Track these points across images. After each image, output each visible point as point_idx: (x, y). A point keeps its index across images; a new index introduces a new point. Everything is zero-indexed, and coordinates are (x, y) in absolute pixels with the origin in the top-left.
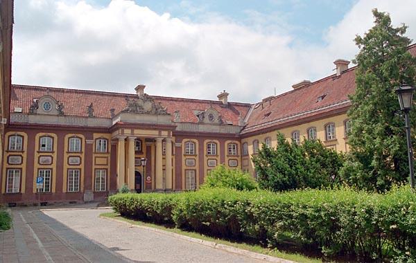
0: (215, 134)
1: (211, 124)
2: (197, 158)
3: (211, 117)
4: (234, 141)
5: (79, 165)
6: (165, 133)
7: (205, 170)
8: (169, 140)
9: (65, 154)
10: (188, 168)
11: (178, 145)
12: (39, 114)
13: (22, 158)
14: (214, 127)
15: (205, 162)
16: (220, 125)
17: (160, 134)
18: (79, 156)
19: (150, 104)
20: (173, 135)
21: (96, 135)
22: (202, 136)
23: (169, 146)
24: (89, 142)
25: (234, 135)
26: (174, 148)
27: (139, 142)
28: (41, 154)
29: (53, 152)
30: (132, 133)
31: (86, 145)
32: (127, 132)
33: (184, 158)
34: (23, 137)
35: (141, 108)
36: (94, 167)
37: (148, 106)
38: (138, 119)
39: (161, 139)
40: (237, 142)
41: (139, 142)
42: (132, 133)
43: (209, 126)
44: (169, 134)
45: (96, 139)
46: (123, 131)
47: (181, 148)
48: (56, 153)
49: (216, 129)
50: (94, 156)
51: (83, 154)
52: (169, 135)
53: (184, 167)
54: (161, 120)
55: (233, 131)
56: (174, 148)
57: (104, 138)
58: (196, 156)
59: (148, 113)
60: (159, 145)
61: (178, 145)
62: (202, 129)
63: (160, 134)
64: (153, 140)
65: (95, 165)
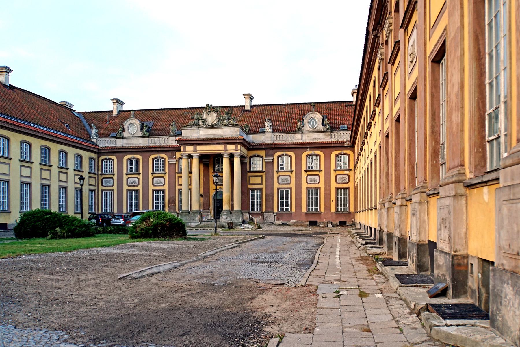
4: (345, 152)
5: (163, 185)
6: (231, 148)
10: (281, 186)
11: (269, 159)
12: (125, 138)
13: (113, 179)
14: (316, 135)
15: (293, 180)
16: (324, 132)
17: (226, 150)
18: (163, 177)
19: (215, 115)
23: (237, 162)
25: (343, 143)
26: (264, 163)
27: (204, 159)
28: (338, 173)
29: (320, 171)
30: (195, 151)
33: (276, 175)
34: (290, 156)
35: (204, 121)
37: (212, 118)
38: (203, 133)
40: (348, 152)
41: (204, 159)
42: (195, 151)
43: (311, 135)
44: (236, 147)
46: (185, 149)
48: (116, 175)
53: (276, 186)
56: (264, 163)
59: (212, 126)
60: (226, 162)
61: (269, 159)
62: (298, 138)
63: (226, 150)
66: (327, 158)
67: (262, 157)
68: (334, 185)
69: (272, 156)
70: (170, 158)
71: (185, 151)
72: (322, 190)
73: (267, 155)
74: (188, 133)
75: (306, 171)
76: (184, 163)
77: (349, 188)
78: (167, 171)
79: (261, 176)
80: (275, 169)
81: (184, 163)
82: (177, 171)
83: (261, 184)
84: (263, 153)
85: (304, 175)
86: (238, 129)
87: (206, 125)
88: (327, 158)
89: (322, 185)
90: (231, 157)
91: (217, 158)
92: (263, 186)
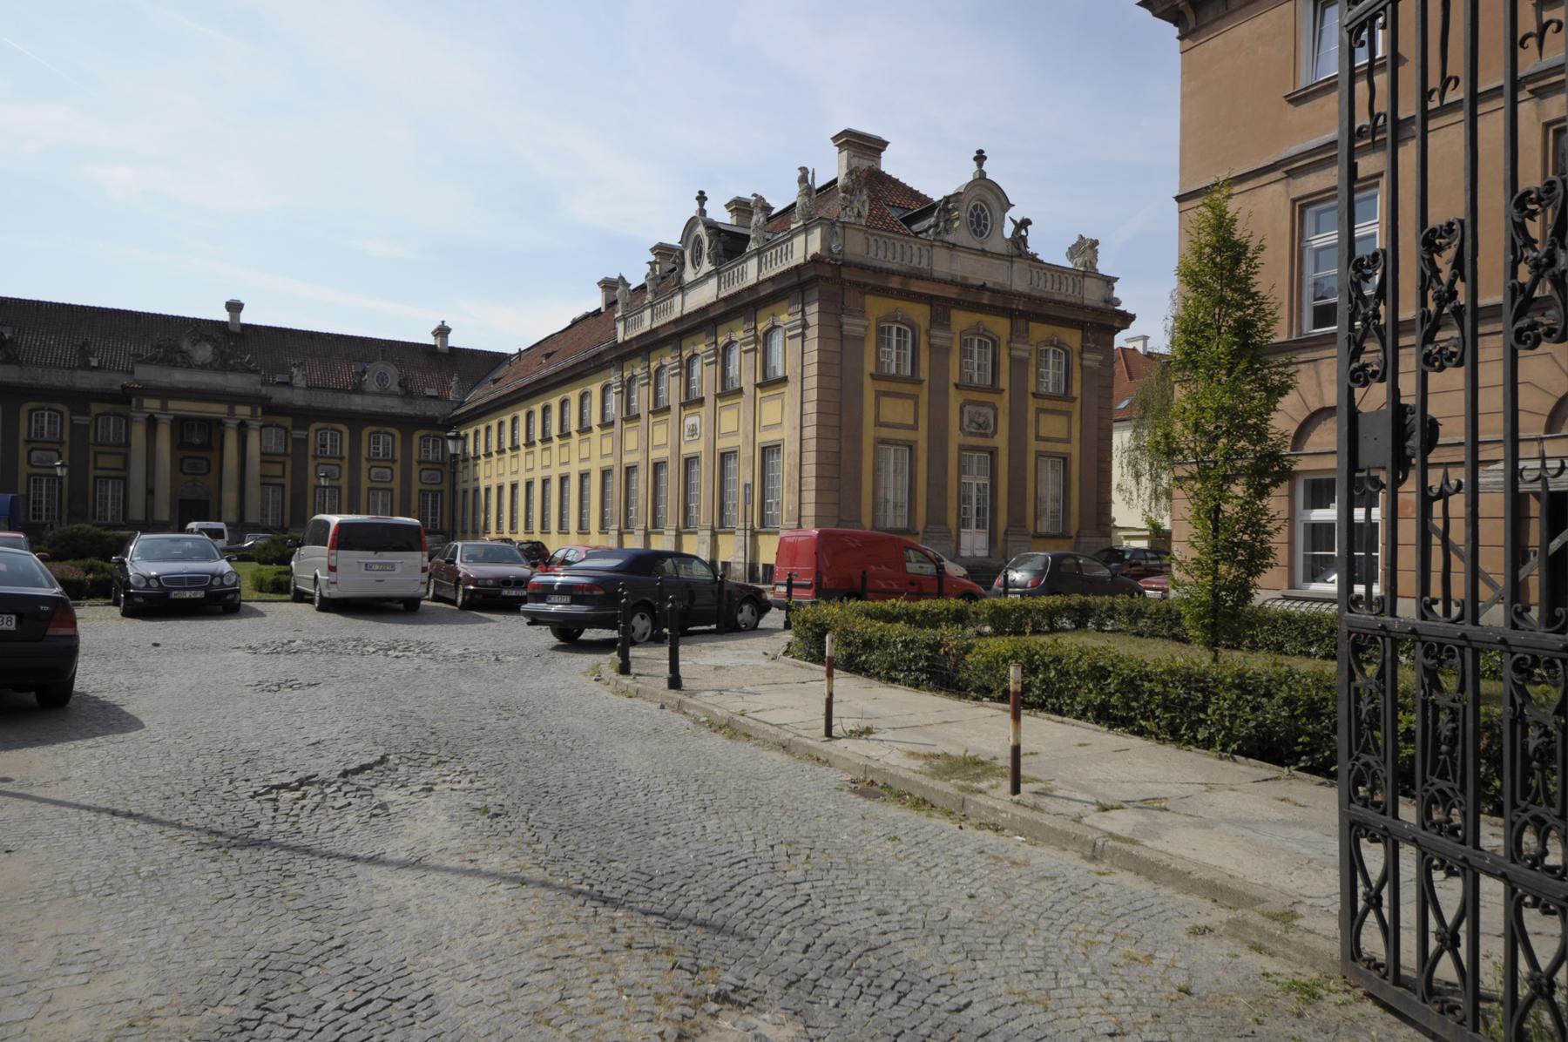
0: (392, 415)
1: (380, 394)
2: (345, 465)
3: (382, 378)
6: (243, 411)
7: (364, 492)
8: (255, 424)
9: (22, 445)
11: (300, 434)
16: (402, 397)
17: (231, 413)
20: (264, 412)
21: (95, 408)
22: (357, 420)
24: (80, 420)
25: (436, 419)
27: (182, 425)
30: (164, 408)
31: (73, 427)
32: (152, 404)
33: (311, 464)
36: (92, 473)
37: (204, 352)
38: (179, 378)
39: (232, 423)
41: (182, 425)
42: (164, 408)
45: (97, 416)
47: (305, 441)
49: (395, 406)
50: (92, 450)
51: (67, 446)
52: (254, 415)
54: (235, 382)
55: (435, 410)
57: (116, 415)
58: (342, 458)
59: (203, 367)
61: (300, 434)
62: (358, 403)
64: (220, 423)
65: (96, 468)
66: (407, 442)
67: (285, 429)
68: (416, 486)
69: (306, 428)
70: (73, 412)
71: (140, 407)
72: (397, 493)
73: (294, 428)
74: (148, 374)
75: (368, 460)
76: (138, 433)
77: (441, 492)
78: (66, 437)
79: (283, 463)
80: (311, 452)
81: (138, 433)
82: (92, 440)
83: (283, 476)
84: (287, 422)
85: (365, 465)
86: (254, 378)
87: (188, 364)
88: (407, 442)
89: (396, 485)
90: (243, 428)
91: (213, 427)
92: (287, 481)
